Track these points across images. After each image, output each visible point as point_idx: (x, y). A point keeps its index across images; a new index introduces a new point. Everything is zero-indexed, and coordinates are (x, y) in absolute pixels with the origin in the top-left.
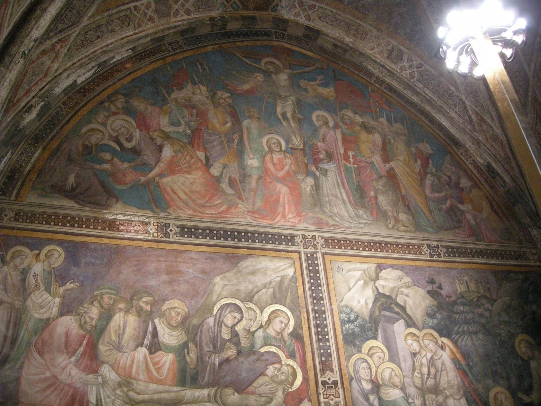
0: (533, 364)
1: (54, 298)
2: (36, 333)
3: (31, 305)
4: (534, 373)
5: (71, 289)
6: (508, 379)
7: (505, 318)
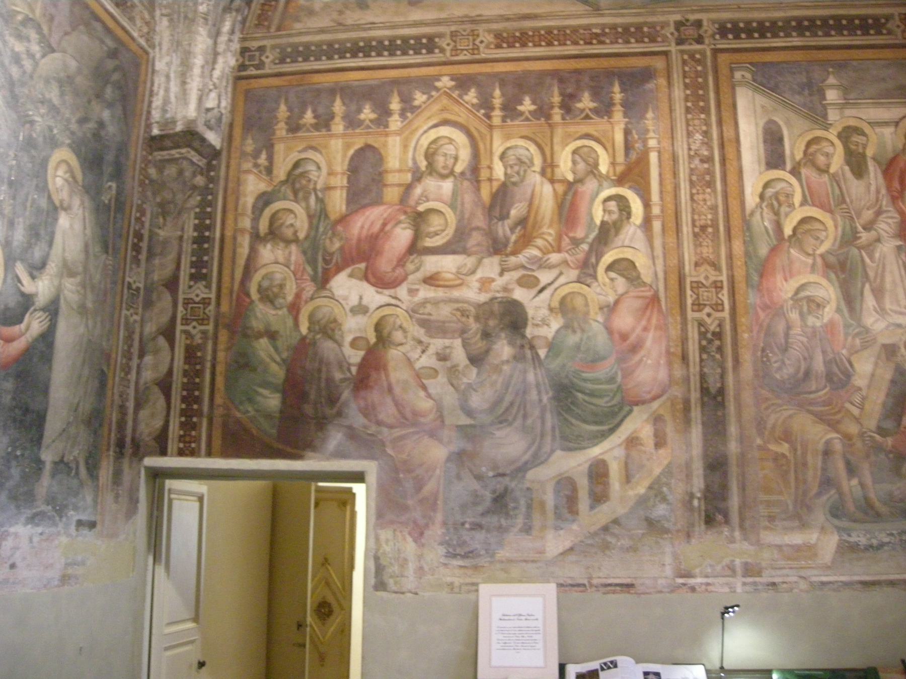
0: (64, 221)
4: (58, 239)
6: (11, 224)
7: (54, 95)
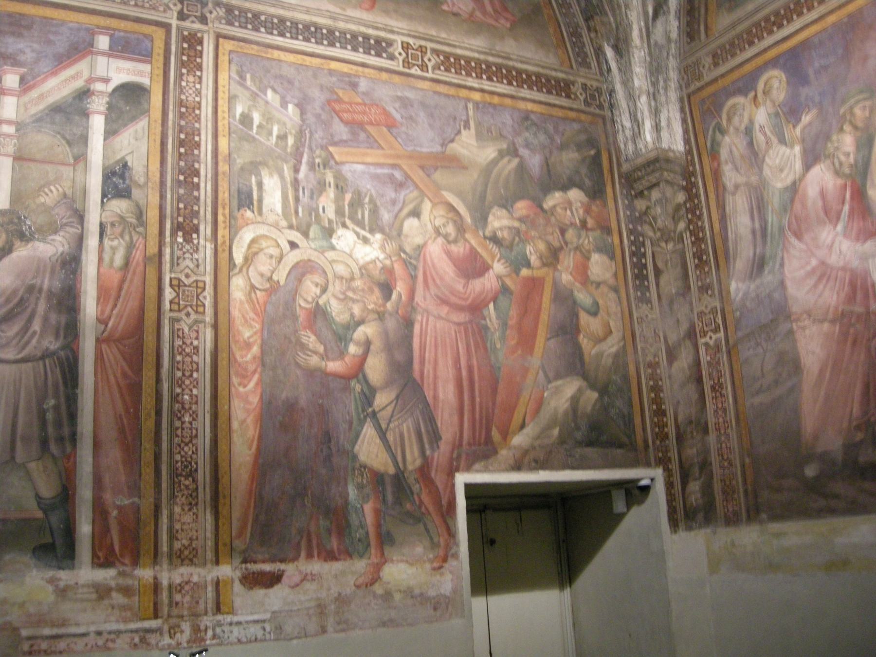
1: (792, 147)
2: (785, 210)
3: (769, 173)
5: (810, 124)
